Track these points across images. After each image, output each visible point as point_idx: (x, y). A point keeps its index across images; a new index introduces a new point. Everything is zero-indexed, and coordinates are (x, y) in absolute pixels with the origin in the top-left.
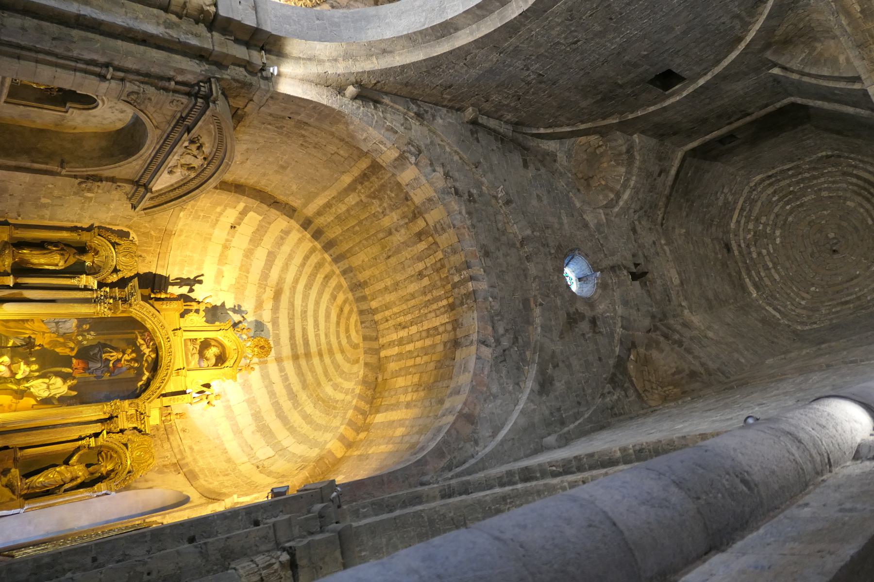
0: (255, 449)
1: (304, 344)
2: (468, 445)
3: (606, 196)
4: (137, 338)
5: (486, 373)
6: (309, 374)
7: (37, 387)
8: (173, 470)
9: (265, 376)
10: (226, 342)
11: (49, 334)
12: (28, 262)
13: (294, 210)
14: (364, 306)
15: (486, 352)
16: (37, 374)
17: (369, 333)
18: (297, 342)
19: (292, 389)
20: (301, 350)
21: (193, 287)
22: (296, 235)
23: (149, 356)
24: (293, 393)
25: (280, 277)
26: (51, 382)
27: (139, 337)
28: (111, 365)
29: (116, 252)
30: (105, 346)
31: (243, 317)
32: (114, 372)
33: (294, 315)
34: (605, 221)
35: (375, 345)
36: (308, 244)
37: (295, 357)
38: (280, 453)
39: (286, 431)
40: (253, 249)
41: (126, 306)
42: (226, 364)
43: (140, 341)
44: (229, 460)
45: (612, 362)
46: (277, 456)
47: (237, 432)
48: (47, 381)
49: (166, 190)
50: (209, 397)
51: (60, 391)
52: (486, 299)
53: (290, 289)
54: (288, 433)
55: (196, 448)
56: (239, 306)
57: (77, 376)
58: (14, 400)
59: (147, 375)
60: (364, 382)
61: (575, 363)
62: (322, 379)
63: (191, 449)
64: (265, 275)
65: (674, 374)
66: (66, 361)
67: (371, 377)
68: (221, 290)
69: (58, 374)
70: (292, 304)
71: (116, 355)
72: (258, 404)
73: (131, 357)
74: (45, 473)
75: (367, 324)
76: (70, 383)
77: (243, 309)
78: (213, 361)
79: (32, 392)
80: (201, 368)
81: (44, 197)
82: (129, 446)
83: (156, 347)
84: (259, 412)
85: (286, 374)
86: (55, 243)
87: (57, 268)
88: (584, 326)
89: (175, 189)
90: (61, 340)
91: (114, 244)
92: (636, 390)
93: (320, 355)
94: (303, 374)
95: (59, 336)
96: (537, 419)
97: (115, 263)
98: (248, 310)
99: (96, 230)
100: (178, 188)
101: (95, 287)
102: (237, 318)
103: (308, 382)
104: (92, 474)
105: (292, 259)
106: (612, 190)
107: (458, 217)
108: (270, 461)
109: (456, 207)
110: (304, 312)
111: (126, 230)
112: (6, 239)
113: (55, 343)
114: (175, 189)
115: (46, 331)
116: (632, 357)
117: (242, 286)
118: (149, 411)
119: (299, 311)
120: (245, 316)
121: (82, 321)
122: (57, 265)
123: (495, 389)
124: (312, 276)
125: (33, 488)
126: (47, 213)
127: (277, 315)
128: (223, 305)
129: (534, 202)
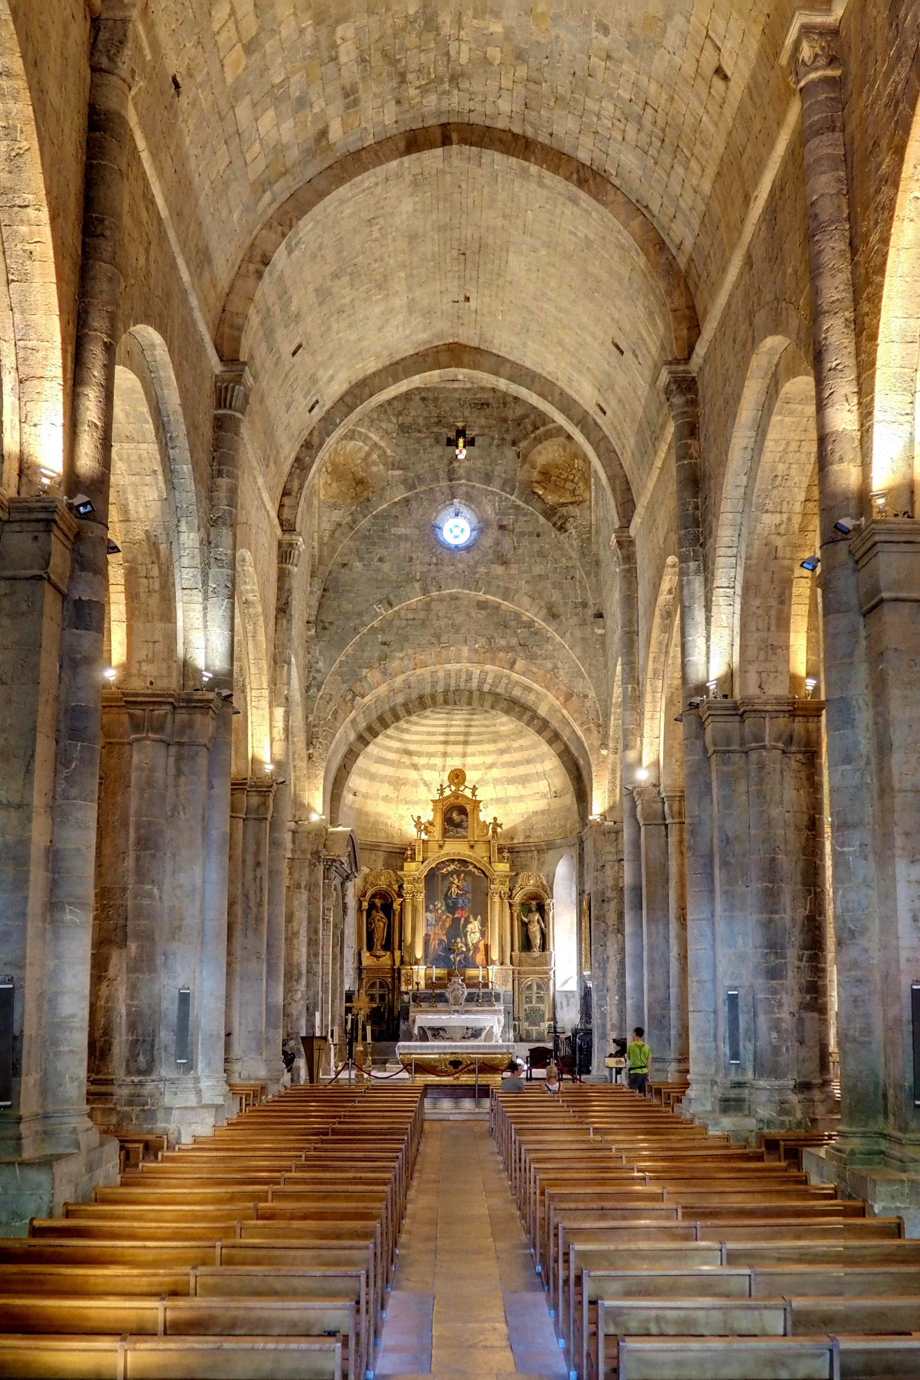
2: (587, 705)
3: (375, 463)
5: (536, 670)
9: (476, 767)
13: (350, 751)
14: (440, 699)
15: (520, 664)
17: (464, 699)
20: (461, 738)
22: (371, 748)
30: (446, 895)
34: (400, 472)
35: (476, 695)
36: (380, 739)
37: (466, 743)
44: (543, 812)
45: (542, 519)
47: (521, 798)
52: (476, 651)
54: (531, 765)
60: (507, 712)
61: (537, 570)
62: (493, 729)
64: (392, 764)
65: (565, 451)
66: (456, 921)
67: (503, 705)
70: (418, 742)
71: (454, 889)
75: (457, 698)
88: (507, 543)
92: (572, 503)
93: (469, 726)
96: (578, 634)
106: (368, 455)
107: (406, 662)
109: (397, 662)
110: (428, 733)
116: (540, 492)
121: (427, 910)
123: (549, 665)
124: (403, 731)
129: (386, 567)
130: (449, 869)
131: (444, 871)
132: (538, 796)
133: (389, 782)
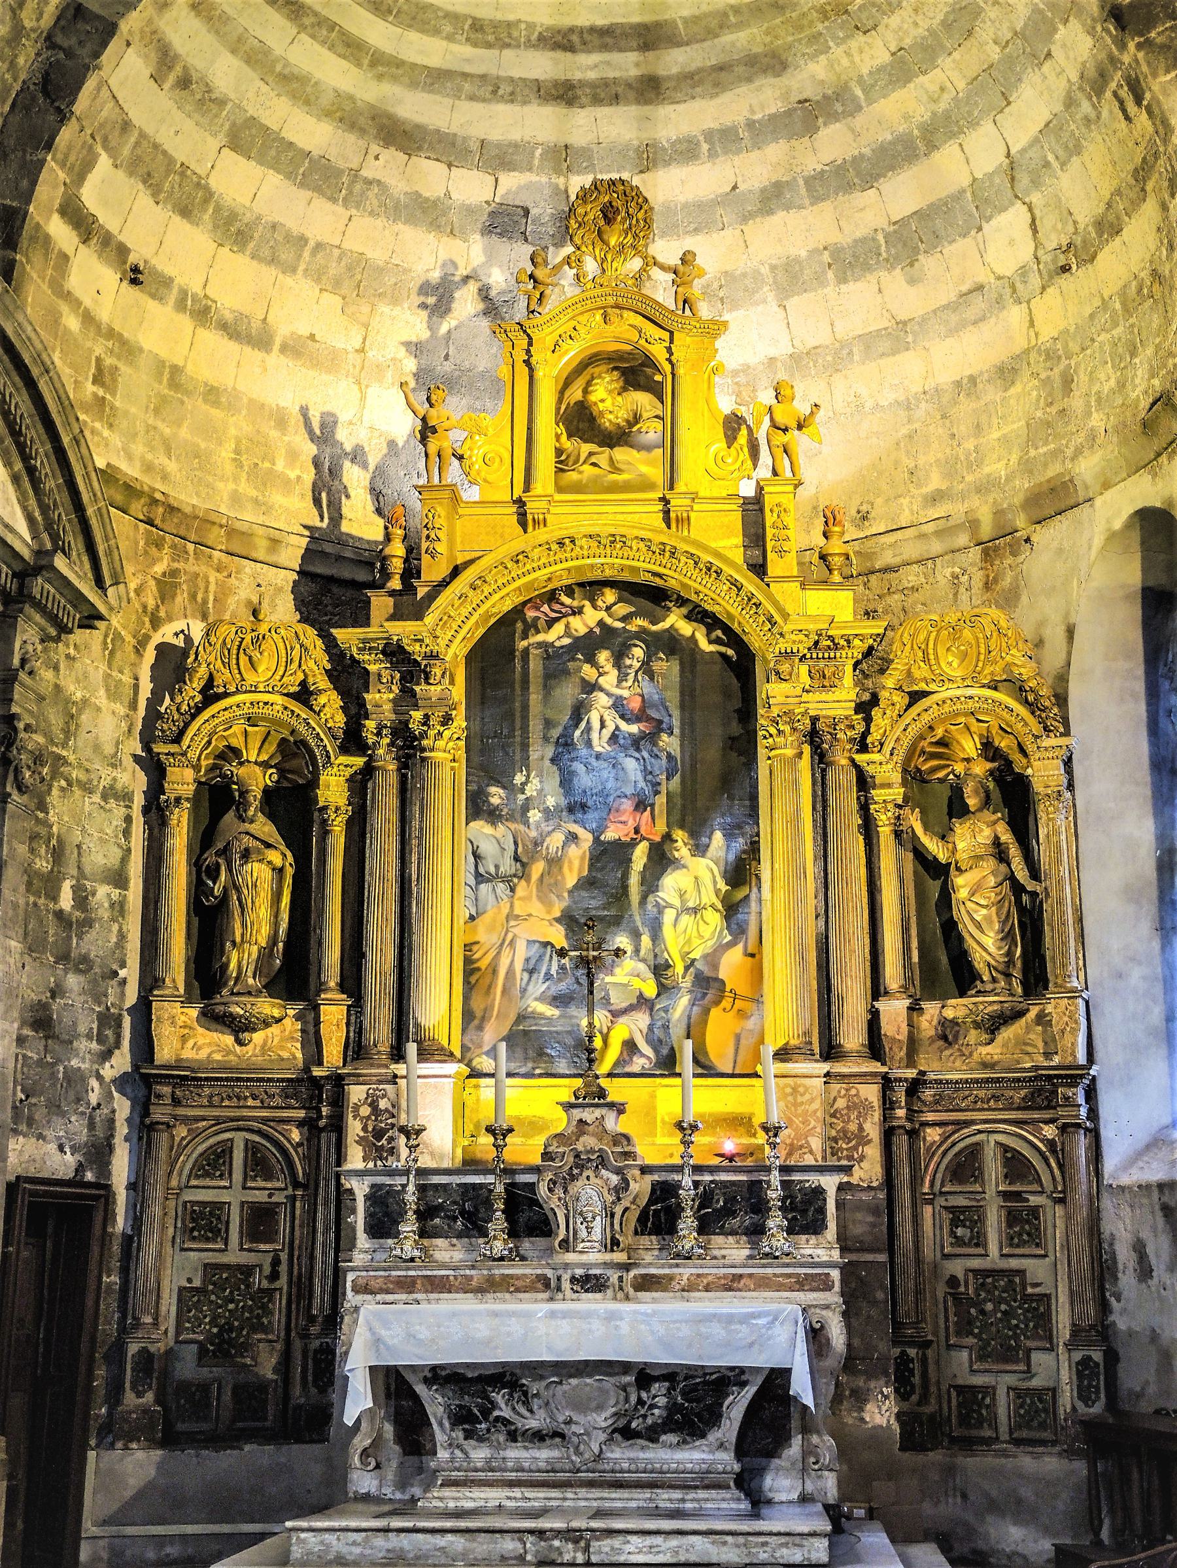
0: (981, 279)
1: (605, 48)
4: (544, 645)
6: (727, 38)
7: (688, 941)
8: (1009, 560)
10: (572, 352)
11: (517, 903)
12: (266, 954)
16: (646, 940)
18: (592, 75)
19: (773, 118)
21: (348, 447)
23: (608, 609)
24: (789, 113)
25: (328, 114)
26: (676, 902)
27: (540, 638)
28: (634, 729)
29: (238, 692)
31: (466, 279)
32: (660, 722)
33: (483, 77)
38: (1024, 180)
39: (936, 156)
40: (218, 209)
41: (437, 671)
42: (658, 352)
43: (555, 635)
44: (1006, 373)
46: (1036, 198)
48: (669, 916)
49: (32, 502)
50: (780, 419)
51: (706, 878)
53: (380, 77)
55: (936, 482)
56: (425, 288)
57: (661, 827)
58: (726, 1003)
59: (676, 621)
63: (935, 498)
68: (362, 350)
69: (650, 883)
72: (803, 254)
73: (608, 667)
74: (966, 927)
76: (682, 847)
77: (435, 276)
78: (642, 400)
79: (705, 957)
80: (671, 446)
81: (55, 898)
82: (923, 686)
83: (581, 585)
84: (836, 252)
85: (709, 135)
86: (201, 874)
87: (290, 872)
89: (31, 471)
90: (538, 868)
91: (210, 695)
94: (721, 68)
95: (524, 875)
97: (278, 699)
98: (443, 256)
99: (159, 748)
100: (26, 458)
101: (359, 761)
102: (466, 303)
103: (757, 49)
104: (987, 802)
105: (267, 51)
108: (1047, 223)
111: (150, 655)
112: (194, 1013)
113: (547, 885)
114: (31, 471)
115: (505, 910)
117: (349, 268)
118: (814, 618)
119: (467, 50)
120: (462, 272)
121: (477, 807)
122: (280, 871)
125: (1010, 963)
126: (103, 893)
127: (474, 146)
128: (415, 348)
130: (579, 626)
131: (555, 635)
132: (978, 304)
133: (317, 275)
